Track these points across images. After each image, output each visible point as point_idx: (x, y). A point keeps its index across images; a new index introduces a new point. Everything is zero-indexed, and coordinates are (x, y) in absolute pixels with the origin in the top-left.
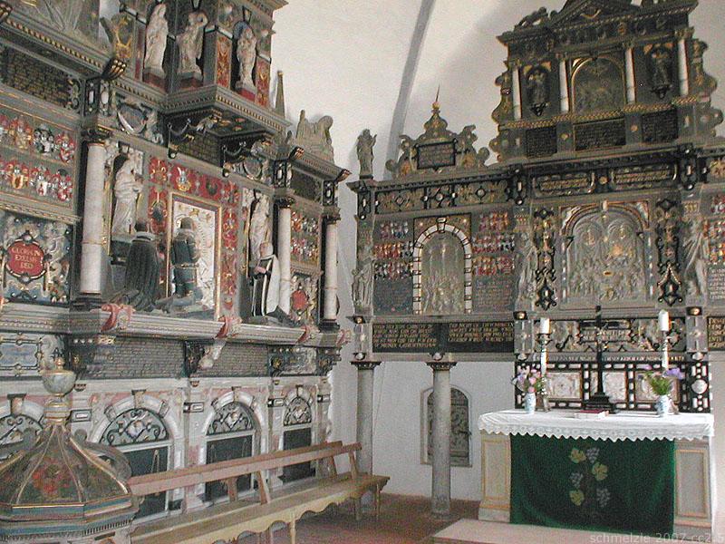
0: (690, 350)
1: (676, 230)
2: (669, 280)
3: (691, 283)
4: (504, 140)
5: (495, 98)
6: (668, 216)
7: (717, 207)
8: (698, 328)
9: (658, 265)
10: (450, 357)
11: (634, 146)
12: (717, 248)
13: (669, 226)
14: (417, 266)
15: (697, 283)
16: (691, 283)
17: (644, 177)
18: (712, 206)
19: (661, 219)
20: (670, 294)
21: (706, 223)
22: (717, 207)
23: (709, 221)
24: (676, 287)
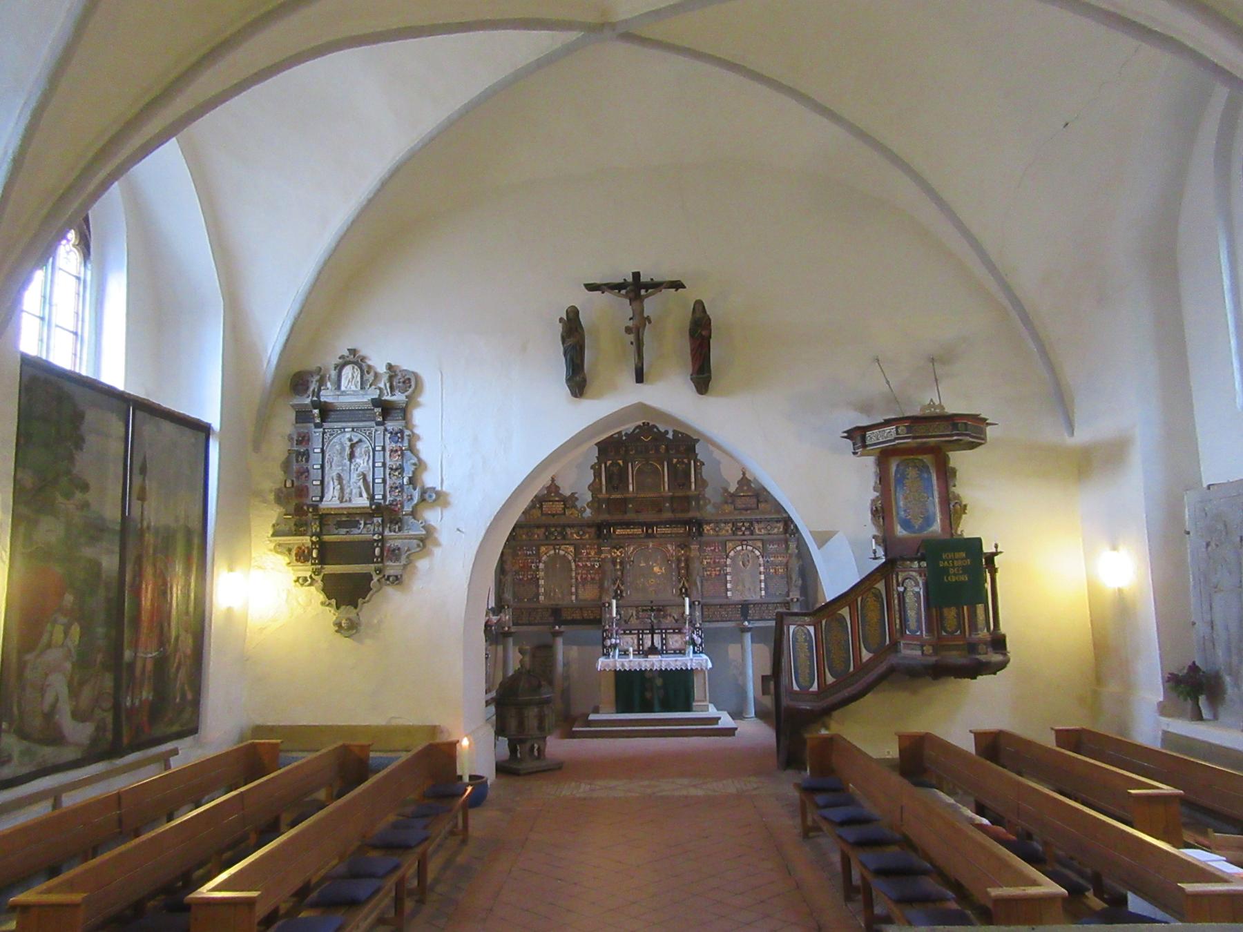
1: (687, 560)
4: (596, 503)
5: (590, 477)
10: (563, 628)
11: (667, 515)
14: (542, 574)
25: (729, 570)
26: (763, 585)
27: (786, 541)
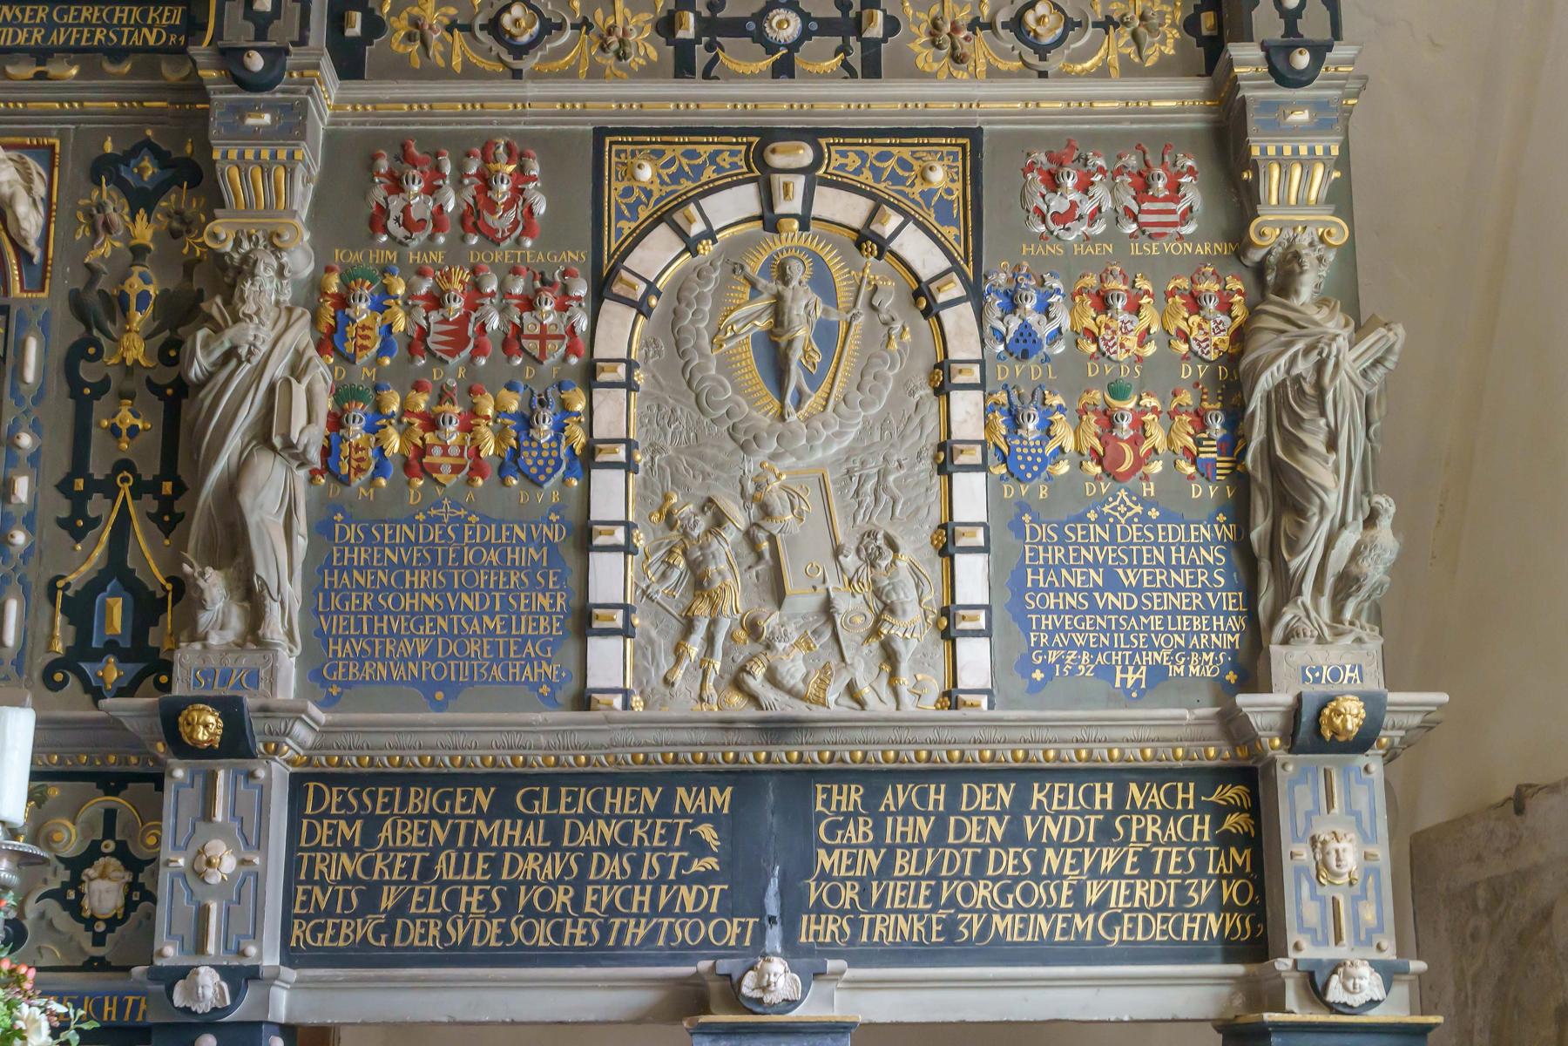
0: (170, 953)
2: (116, 569)
3: (215, 586)
6: (144, 231)
7: (396, 204)
8: (222, 832)
9: (65, 487)
12: (378, 409)
13: (143, 284)
15: (251, 597)
16: (215, 586)
17: (49, 26)
18: (379, 194)
19: (105, 248)
20: (111, 646)
21: (334, 284)
22: (396, 204)
23: (349, 277)
24: (146, 609)
25: (611, 413)
26: (973, 579)
27: (1227, 144)
